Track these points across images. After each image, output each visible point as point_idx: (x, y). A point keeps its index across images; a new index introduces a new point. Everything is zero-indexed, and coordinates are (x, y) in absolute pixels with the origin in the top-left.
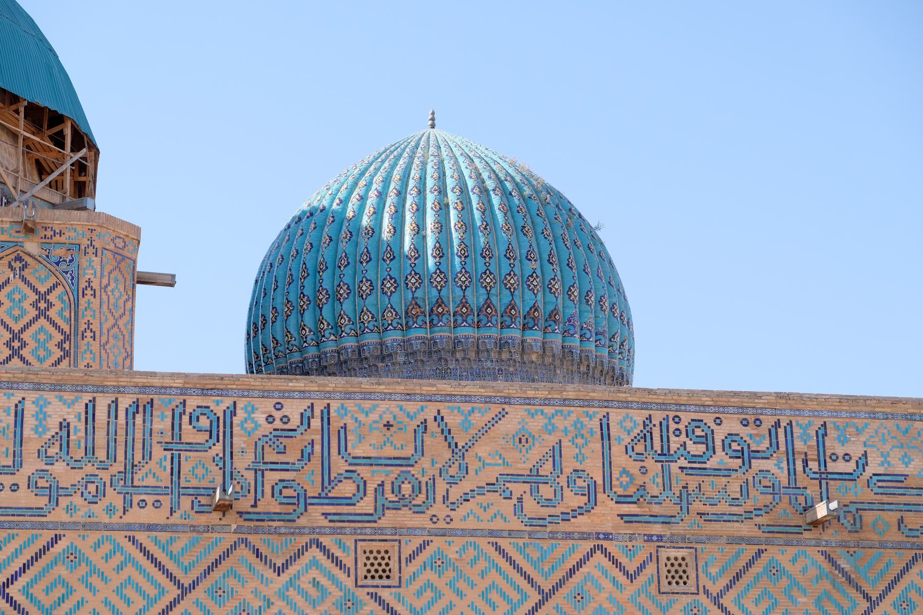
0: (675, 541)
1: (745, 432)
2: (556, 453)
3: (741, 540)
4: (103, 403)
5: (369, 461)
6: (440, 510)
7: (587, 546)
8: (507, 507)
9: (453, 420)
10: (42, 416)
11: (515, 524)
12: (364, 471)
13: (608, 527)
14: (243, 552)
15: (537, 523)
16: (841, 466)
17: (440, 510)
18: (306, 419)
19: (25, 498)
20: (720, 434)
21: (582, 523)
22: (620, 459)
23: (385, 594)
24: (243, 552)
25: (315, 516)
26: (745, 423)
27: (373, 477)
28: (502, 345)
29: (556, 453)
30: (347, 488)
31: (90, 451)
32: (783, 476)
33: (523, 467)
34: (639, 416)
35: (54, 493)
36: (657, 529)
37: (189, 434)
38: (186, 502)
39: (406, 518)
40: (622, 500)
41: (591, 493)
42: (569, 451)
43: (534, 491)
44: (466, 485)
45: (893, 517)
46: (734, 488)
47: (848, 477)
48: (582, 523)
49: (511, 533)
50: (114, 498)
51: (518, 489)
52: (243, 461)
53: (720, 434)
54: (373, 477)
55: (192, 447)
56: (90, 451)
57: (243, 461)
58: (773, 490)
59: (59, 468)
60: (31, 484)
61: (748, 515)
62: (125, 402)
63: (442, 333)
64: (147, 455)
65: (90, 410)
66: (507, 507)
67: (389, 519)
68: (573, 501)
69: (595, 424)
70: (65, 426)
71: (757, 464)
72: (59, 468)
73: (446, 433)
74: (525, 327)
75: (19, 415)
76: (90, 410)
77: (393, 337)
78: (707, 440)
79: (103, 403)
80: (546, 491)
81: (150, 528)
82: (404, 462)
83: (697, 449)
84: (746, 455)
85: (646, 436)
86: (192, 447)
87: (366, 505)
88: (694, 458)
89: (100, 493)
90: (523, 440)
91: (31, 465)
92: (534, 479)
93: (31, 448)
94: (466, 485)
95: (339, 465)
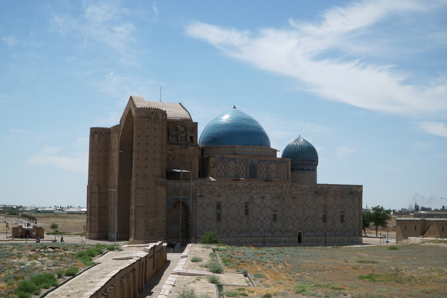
0: (343, 195)
1: (347, 187)
2: (336, 189)
3: (346, 195)
4: (310, 186)
5: (325, 190)
6: (329, 193)
7: (337, 195)
8: (333, 193)
9: (330, 187)
10: (306, 187)
11: (334, 194)
12: (325, 190)
13: (339, 194)
14: (318, 196)
15: (335, 194)
16: (353, 190)
17: (329, 193)
18: (321, 187)
19: (306, 192)
20: (346, 187)
21: (337, 194)
22: (340, 190)
23: (326, 199)
24: (318, 196)
25: (322, 193)
26: (347, 187)
27: (325, 191)
28: (311, 163)
29: (336, 189)
30: (324, 192)
31: (309, 189)
32: (349, 190)
33: (334, 190)
34: (341, 186)
35: (307, 192)
36: (342, 194)
37: (315, 188)
38: (314, 192)
39: (327, 193)
40: (340, 192)
41: (338, 192)
42: (337, 189)
43: (335, 191)
44: (331, 191)
45: (355, 193)
46: (346, 191)
47: (353, 191)
48: (337, 194)
49: (333, 195)
50: (310, 192)
51: (334, 191)
52: (318, 190)
53: (346, 187)
54: (325, 191)
55: (315, 189)
56: (309, 189)
57: (318, 190)
58: (349, 191)
59: (307, 190)
60: (306, 191)
61: (347, 193)
62: (311, 186)
63: (306, 162)
64: (312, 189)
65: (309, 186)
66: (333, 193)
67: (326, 194)
68: (337, 192)
69: (338, 187)
70: (308, 187)
71: (348, 190)
72: (307, 190)
73: (330, 188)
74: (312, 162)
75: (305, 186)
76: (309, 186)
77: (302, 162)
78: (345, 188)
79: (310, 186)
80: (335, 192)
81: (312, 194)
82: (327, 190)
83: (344, 189)
84: (347, 189)
85: (341, 188)
86: (315, 189)
87: (325, 193)
88: (344, 189)
89: (310, 192)
90: (334, 188)
91: (306, 190)
92: (335, 191)
93: (306, 189)
94: (331, 191)
95: (323, 190)
